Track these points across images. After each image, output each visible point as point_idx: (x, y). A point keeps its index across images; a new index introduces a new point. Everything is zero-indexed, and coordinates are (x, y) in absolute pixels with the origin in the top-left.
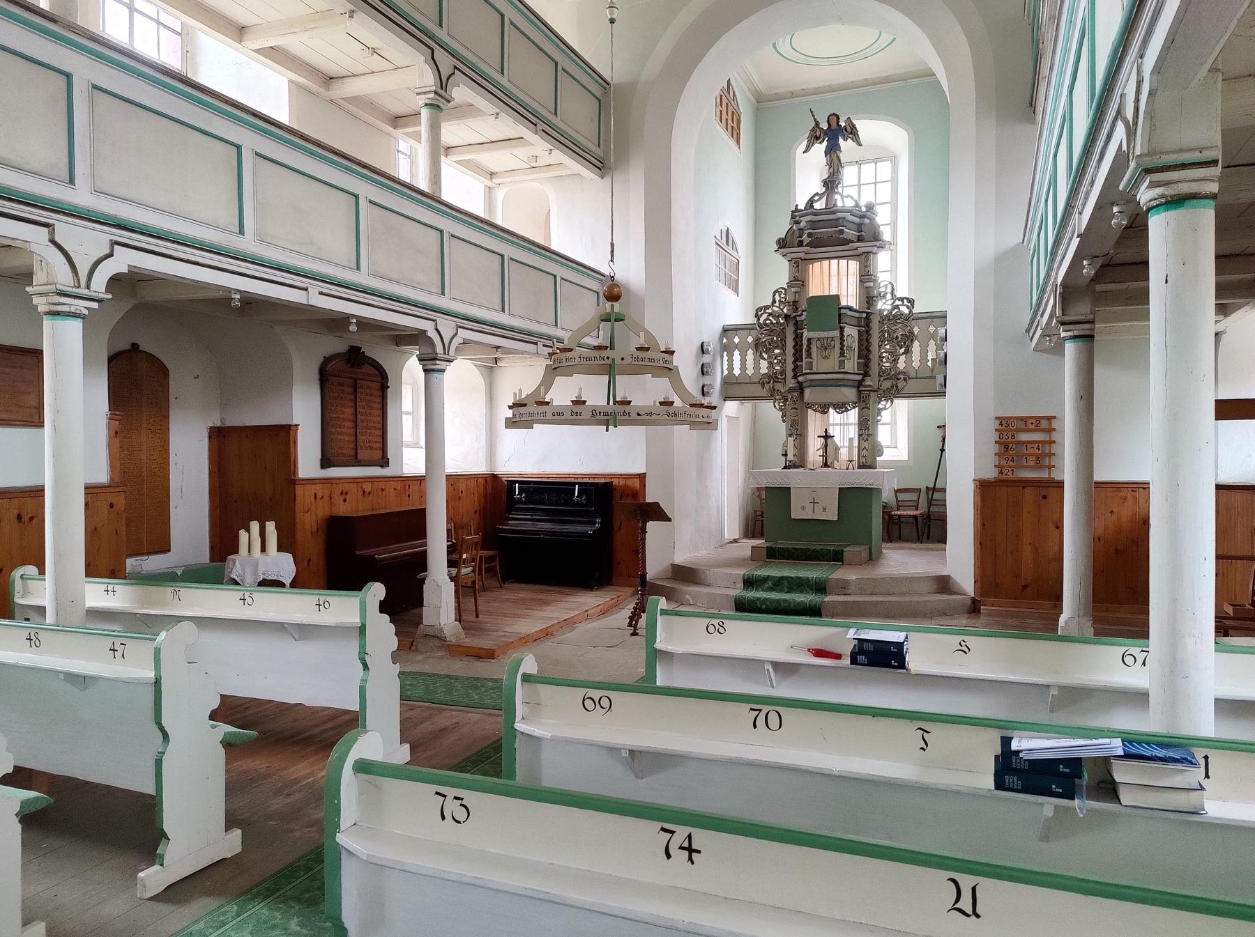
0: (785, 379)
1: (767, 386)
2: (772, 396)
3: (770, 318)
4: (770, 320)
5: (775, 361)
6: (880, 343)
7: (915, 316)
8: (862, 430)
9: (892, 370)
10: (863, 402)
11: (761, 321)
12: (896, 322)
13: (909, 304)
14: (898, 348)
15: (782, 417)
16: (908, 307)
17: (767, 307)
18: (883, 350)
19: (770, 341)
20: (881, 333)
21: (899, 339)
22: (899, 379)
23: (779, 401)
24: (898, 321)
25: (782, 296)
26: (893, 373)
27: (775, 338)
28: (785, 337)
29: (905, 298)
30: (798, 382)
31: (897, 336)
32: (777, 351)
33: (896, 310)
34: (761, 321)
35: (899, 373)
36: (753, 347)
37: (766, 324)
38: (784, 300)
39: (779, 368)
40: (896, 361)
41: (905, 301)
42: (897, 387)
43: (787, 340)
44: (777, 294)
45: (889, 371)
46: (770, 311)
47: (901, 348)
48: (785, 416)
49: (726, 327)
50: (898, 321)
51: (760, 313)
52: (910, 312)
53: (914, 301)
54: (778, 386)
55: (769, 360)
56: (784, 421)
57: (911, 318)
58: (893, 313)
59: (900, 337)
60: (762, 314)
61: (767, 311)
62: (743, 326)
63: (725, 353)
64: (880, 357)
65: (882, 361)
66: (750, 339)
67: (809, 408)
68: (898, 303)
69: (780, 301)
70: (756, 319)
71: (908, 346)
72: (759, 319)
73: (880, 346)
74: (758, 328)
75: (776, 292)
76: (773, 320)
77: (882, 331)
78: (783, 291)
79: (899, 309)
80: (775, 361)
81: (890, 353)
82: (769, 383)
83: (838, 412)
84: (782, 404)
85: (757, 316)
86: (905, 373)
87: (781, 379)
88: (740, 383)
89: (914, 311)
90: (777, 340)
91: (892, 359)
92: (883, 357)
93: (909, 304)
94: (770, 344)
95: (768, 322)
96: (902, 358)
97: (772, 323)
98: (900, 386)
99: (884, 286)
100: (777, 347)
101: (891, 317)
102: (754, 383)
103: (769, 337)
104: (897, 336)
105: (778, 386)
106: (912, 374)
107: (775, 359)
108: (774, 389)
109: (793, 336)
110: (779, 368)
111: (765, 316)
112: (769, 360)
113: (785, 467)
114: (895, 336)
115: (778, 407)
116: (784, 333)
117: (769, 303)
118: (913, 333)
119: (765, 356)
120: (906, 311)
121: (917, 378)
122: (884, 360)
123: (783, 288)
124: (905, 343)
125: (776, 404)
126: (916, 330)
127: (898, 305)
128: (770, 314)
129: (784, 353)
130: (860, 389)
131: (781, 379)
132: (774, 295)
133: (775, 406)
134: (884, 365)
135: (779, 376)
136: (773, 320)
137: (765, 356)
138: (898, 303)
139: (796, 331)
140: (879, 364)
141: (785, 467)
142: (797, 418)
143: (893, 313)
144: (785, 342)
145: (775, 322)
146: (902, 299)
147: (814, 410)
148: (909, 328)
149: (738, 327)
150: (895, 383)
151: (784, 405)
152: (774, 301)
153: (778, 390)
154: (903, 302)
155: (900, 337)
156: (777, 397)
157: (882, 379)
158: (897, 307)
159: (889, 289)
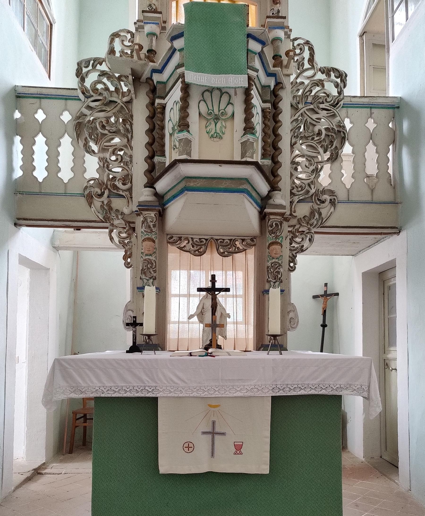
0: (130, 190)
1: (97, 202)
2: (107, 219)
3: (105, 80)
4: (104, 84)
5: (113, 158)
6: (293, 141)
7: (346, 100)
8: (269, 282)
9: (312, 186)
10: (271, 232)
11: (88, 83)
12: (318, 107)
13: (339, 80)
14: (321, 150)
15: (125, 258)
16: (337, 86)
17: (98, 61)
18: (297, 152)
19: (104, 121)
20: (295, 124)
21: (323, 136)
22: (323, 202)
23: (121, 230)
24: (322, 106)
25: (127, 43)
26: (313, 191)
27: (113, 120)
28: (132, 116)
29: (335, 70)
30: (156, 194)
31: (320, 130)
32: (117, 140)
33: (318, 88)
34: (88, 83)
35: (324, 192)
36: (71, 128)
37: (95, 90)
38: (129, 52)
39: (119, 170)
40: (317, 171)
41: (333, 74)
42: (320, 214)
43: (135, 122)
44: (117, 41)
45: (307, 188)
46: (104, 67)
47: (325, 152)
48: (130, 257)
49: (21, 90)
50: (322, 106)
51: (85, 70)
52: (340, 93)
53: (346, 76)
54: (117, 203)
55: (102, 155)
56: (128, 265)
57: (341, 103)
58: (313, 94)
59: (324, 132)
60: (88, 73)
61: (98, 67)
62: (54, 92)
63: (18, 139)
64: (293, 162)
65: (296, 169)
66: (66, 117)
67: (173, 243)
68: (320, 76)
69: (122, 52)
70: (77, 80)
71: (336, 147)
72: (83, 80)
73: (292, 146)
74: (82, 96)
75: (115, 35)
76: (109, 84)
77: (297, 120)
78: (129, 36)
79: (323, 86)
80: (113, 158)
81: (310, 159)
82: (101, 195)
83: (222, 254)
84: (124, 235)
85: (79, 73)
86: (332, 193)
87: (123, 191)
88: (46, 194)
89: (347, 92)
90: (117, 121)
91: (312, 168)
92: (298, 164)
93: (339, 80)
94: (103, 127)
95: (100, 86)
96: (327, 167)
97: (107, 89)
98: (324, 212)
99: (299, 45)
100: (117, 133)
101: (310, 99)
102: (72, 195)
103: (102, 114)
104: (320, 130)
105: (117, 203)
106: (341, 195)
107: (114, 153)
108: (110, 209)
109: (147, 113)
110: (119, 170)
111: (93, 77)
112: (102, 155)
113: (134, 349)
114: (316, 129)
115: (116, 239)
116: (130, 110)
117: (102, 53)
118: (344, 127)
119: (95, 147)
120: (334, 92)
121: (348, 201)
122: (300, 169)
123: (129, 32)
124: (332, 143)
125: (114, 235)
126: (348, 124)
127: (321, 80)
128: (103, 74)
129: (129, 145)
130: (267, 210)
131: (123, 191)
132: (112, 41)
133: (111, 239)
134: (300, 176)
135: (119, 184)
136: (109, 84)
137: (95, 147)
138: (320, 76)
139: (152, 103)
140: (292, 175)
141: (134, 349)
142: (152, 258)
143: (313, 94)
144: (131, 125)
145: (112, 89)
146: (327, 71)
147: (181, 249)
148: (338, 118)
149: (44, 91)
150: (316, 207)
151: (129, 236)
152: (112, 51)
153: (117, 211)
154: (329, 75)
155: (324, 132)
156: (116, 222)
157: (296, 199)
158: (320, 83)
159: (306, 54)
